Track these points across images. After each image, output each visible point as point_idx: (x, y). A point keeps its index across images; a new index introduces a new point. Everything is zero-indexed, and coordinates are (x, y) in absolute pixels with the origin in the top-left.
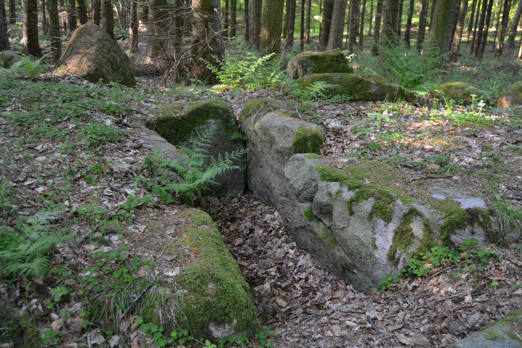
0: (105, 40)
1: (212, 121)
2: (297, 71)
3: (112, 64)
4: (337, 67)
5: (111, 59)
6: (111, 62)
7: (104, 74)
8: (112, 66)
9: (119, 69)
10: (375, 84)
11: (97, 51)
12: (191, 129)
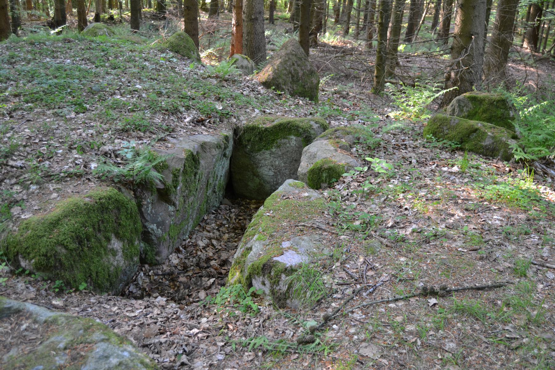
0: (293, 55)
1: (293, 137)
2: (454, 110)
3: (293, 76)
4: (495, 112)
5: (293, 71)
6: (292, 75)
7: (280, 84)
8: (292, 78)
9: (299, 81)
10: (491, 137)
11: (281, 63)
12: (274, 140)
